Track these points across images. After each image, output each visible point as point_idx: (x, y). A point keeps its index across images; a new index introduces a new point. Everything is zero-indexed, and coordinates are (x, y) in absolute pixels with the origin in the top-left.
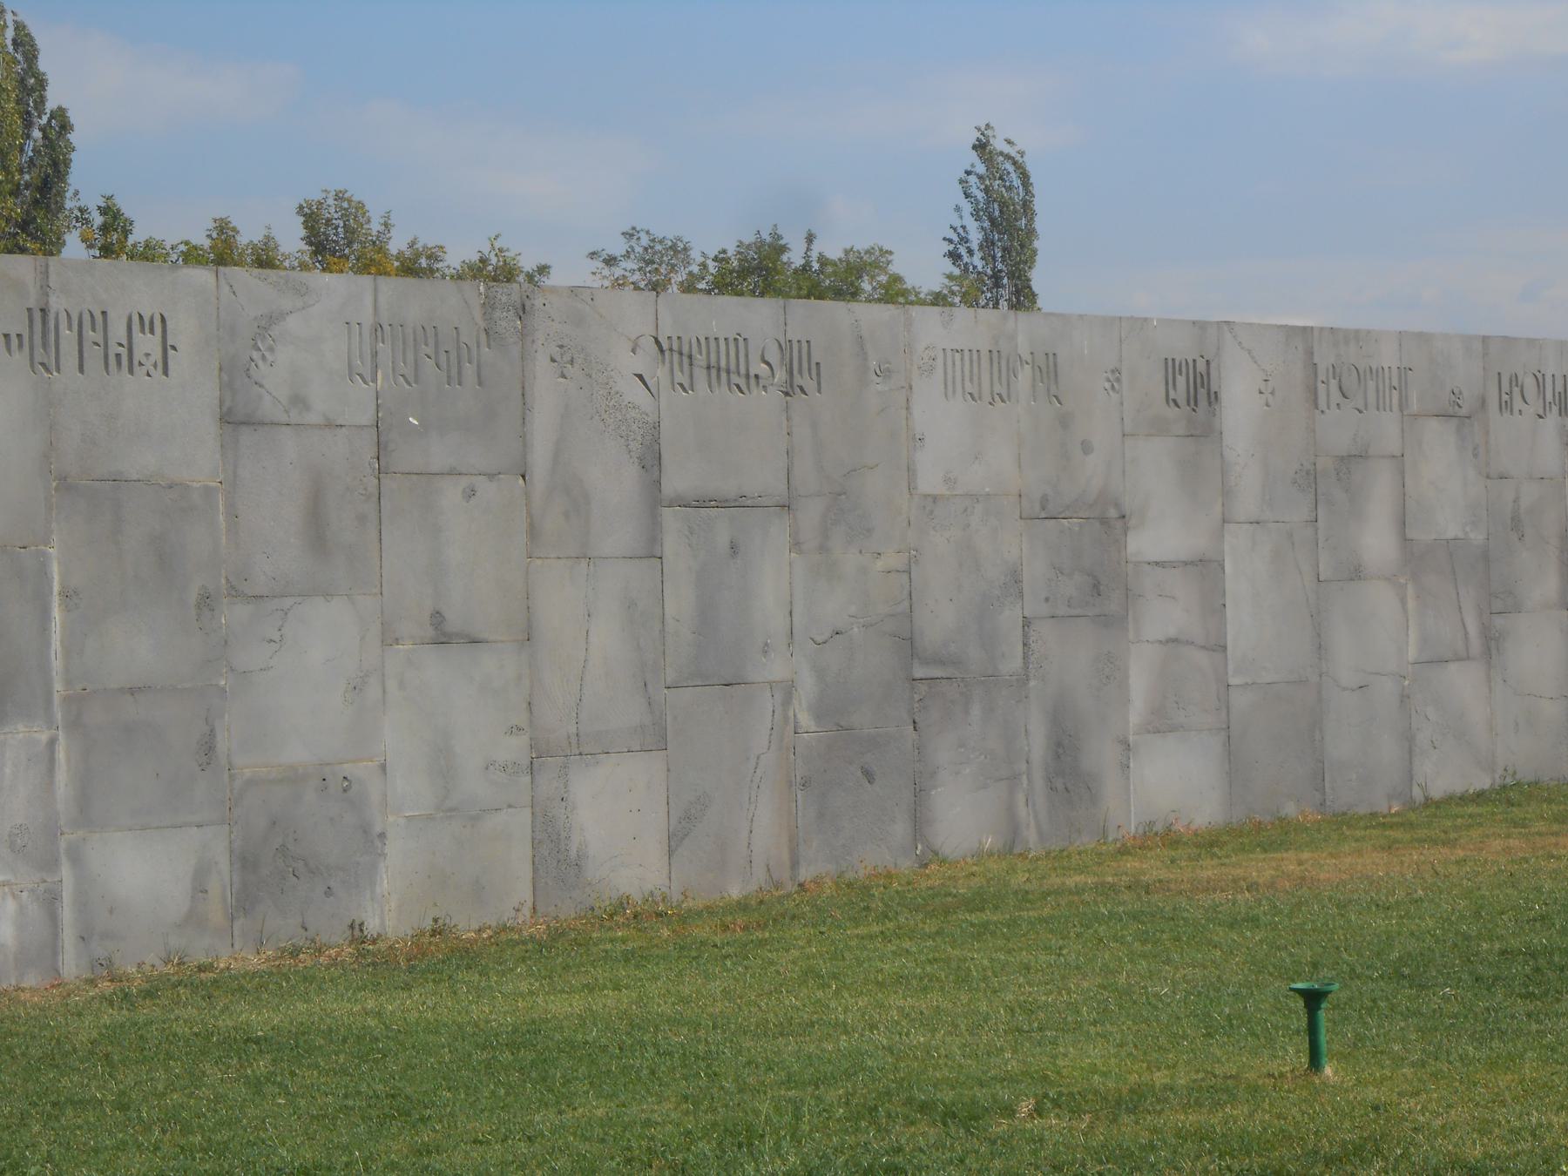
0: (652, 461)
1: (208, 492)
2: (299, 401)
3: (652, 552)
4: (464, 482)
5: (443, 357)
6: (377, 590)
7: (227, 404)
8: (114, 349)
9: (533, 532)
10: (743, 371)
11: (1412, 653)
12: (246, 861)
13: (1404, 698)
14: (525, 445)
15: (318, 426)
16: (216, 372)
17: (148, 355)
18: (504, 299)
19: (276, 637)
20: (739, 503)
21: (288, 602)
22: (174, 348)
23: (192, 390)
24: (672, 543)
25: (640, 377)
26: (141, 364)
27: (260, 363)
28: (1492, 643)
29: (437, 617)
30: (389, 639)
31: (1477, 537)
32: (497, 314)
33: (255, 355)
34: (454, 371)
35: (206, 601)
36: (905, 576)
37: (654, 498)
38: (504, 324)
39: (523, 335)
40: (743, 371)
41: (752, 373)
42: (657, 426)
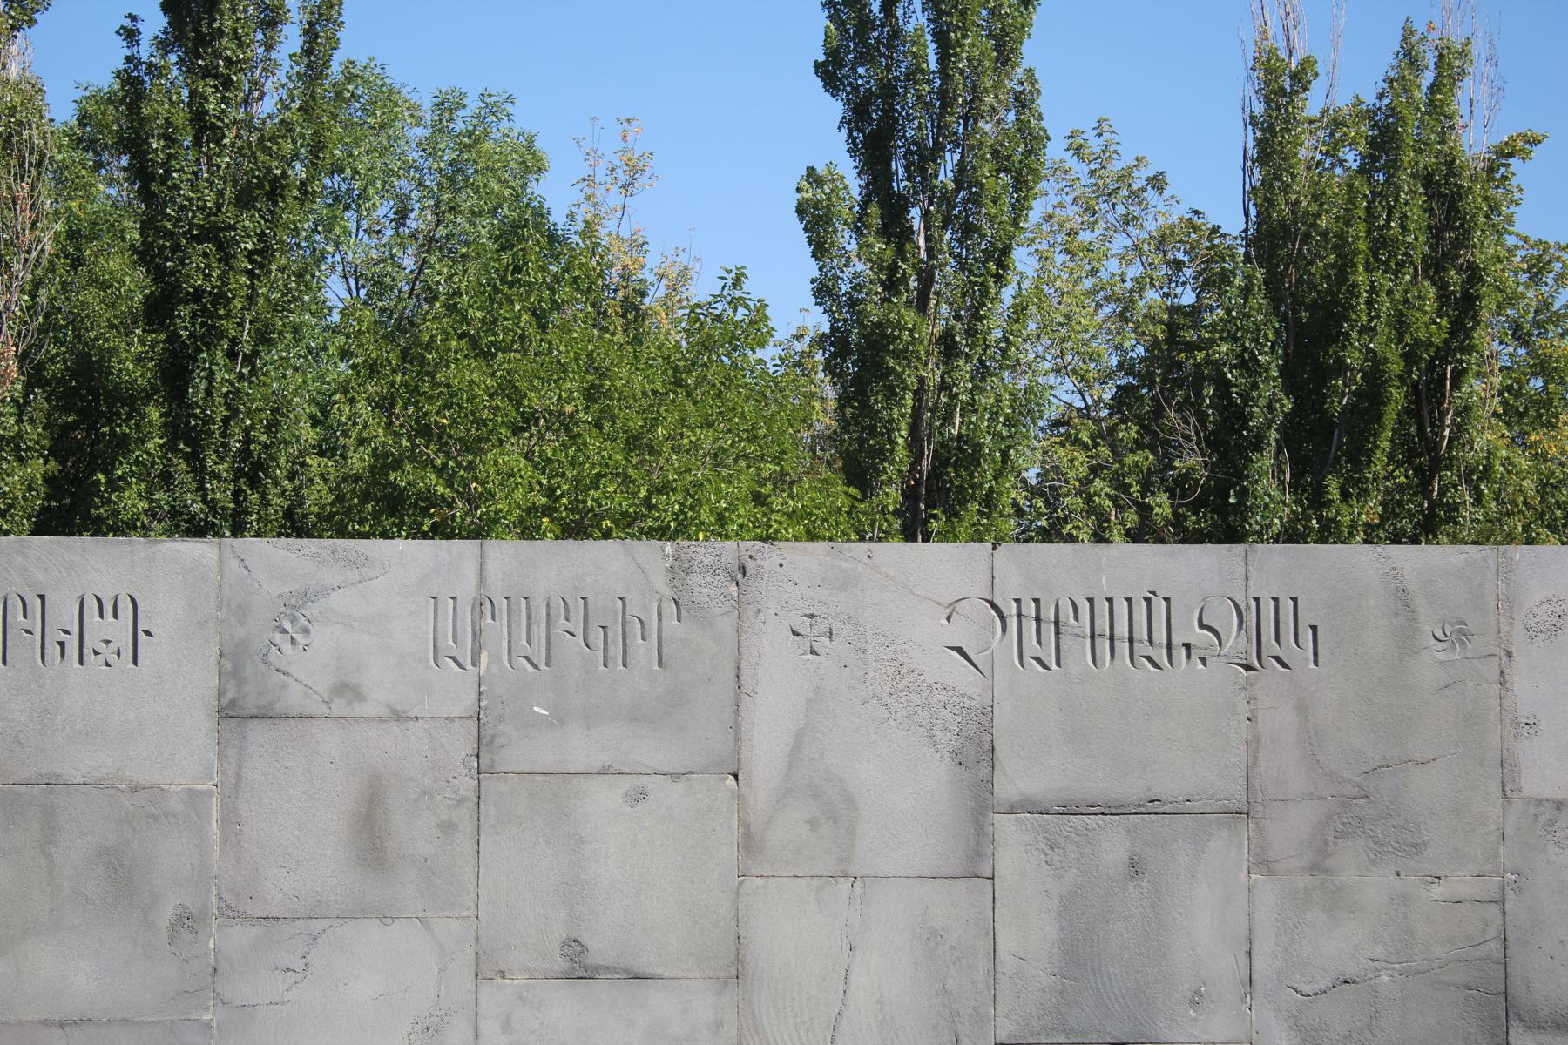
0: (977, 753)
1: (194, 798)
2: (347, 689)
3: (975, 866)
4: (626, 783)
5: (597, 636)
6: (471, 912)
7: (229, 695)
8: (54, 635)
9: (749, 843)
10: (1161, 635)
14: (738, 738)
15: (381, 719)
16: (213, 660)
17: (107, 642)
18: (708, 561)
19: (298, 964)
20: (1151, 807)
21: (317, 926)
22: (148, 633)
23: (180, 678)
25: (960, 650)
26: (96, 653)
27: (287, 647)
29: (574, 948)
30: (486, 968)
32: (695, 579)
33: (278, 638)
34: (616, 651)
35: (187, 922)
36: (1495, 910)
37: (980, 804)
38: (706, 590)
39: (739, 604)
40: (1161, 635)
41: (1177, 640)
42: (988, 712)
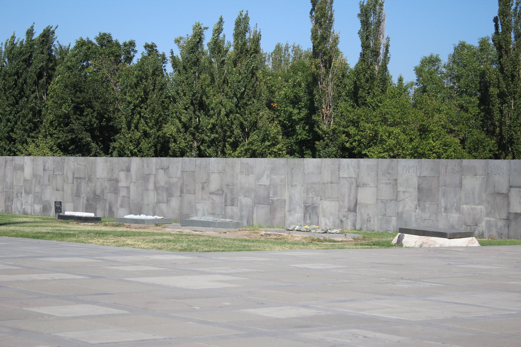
0: (74, 174)
11: (155, 201)
12: (43, 208)
13: (154, 207)
20: (80, 178)
24: (75, 182)
28: (168, 202)
31: (167, 186)
37: (74, 178)
